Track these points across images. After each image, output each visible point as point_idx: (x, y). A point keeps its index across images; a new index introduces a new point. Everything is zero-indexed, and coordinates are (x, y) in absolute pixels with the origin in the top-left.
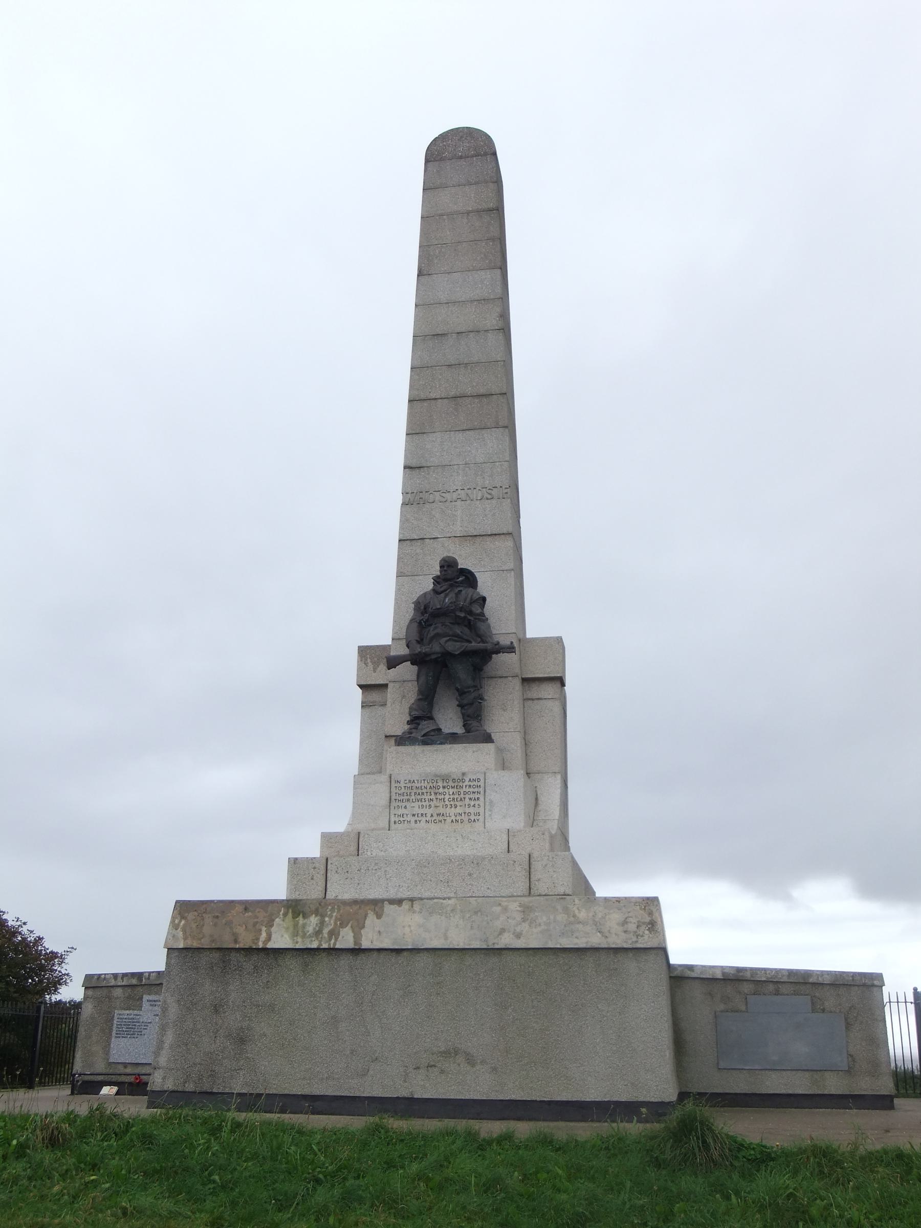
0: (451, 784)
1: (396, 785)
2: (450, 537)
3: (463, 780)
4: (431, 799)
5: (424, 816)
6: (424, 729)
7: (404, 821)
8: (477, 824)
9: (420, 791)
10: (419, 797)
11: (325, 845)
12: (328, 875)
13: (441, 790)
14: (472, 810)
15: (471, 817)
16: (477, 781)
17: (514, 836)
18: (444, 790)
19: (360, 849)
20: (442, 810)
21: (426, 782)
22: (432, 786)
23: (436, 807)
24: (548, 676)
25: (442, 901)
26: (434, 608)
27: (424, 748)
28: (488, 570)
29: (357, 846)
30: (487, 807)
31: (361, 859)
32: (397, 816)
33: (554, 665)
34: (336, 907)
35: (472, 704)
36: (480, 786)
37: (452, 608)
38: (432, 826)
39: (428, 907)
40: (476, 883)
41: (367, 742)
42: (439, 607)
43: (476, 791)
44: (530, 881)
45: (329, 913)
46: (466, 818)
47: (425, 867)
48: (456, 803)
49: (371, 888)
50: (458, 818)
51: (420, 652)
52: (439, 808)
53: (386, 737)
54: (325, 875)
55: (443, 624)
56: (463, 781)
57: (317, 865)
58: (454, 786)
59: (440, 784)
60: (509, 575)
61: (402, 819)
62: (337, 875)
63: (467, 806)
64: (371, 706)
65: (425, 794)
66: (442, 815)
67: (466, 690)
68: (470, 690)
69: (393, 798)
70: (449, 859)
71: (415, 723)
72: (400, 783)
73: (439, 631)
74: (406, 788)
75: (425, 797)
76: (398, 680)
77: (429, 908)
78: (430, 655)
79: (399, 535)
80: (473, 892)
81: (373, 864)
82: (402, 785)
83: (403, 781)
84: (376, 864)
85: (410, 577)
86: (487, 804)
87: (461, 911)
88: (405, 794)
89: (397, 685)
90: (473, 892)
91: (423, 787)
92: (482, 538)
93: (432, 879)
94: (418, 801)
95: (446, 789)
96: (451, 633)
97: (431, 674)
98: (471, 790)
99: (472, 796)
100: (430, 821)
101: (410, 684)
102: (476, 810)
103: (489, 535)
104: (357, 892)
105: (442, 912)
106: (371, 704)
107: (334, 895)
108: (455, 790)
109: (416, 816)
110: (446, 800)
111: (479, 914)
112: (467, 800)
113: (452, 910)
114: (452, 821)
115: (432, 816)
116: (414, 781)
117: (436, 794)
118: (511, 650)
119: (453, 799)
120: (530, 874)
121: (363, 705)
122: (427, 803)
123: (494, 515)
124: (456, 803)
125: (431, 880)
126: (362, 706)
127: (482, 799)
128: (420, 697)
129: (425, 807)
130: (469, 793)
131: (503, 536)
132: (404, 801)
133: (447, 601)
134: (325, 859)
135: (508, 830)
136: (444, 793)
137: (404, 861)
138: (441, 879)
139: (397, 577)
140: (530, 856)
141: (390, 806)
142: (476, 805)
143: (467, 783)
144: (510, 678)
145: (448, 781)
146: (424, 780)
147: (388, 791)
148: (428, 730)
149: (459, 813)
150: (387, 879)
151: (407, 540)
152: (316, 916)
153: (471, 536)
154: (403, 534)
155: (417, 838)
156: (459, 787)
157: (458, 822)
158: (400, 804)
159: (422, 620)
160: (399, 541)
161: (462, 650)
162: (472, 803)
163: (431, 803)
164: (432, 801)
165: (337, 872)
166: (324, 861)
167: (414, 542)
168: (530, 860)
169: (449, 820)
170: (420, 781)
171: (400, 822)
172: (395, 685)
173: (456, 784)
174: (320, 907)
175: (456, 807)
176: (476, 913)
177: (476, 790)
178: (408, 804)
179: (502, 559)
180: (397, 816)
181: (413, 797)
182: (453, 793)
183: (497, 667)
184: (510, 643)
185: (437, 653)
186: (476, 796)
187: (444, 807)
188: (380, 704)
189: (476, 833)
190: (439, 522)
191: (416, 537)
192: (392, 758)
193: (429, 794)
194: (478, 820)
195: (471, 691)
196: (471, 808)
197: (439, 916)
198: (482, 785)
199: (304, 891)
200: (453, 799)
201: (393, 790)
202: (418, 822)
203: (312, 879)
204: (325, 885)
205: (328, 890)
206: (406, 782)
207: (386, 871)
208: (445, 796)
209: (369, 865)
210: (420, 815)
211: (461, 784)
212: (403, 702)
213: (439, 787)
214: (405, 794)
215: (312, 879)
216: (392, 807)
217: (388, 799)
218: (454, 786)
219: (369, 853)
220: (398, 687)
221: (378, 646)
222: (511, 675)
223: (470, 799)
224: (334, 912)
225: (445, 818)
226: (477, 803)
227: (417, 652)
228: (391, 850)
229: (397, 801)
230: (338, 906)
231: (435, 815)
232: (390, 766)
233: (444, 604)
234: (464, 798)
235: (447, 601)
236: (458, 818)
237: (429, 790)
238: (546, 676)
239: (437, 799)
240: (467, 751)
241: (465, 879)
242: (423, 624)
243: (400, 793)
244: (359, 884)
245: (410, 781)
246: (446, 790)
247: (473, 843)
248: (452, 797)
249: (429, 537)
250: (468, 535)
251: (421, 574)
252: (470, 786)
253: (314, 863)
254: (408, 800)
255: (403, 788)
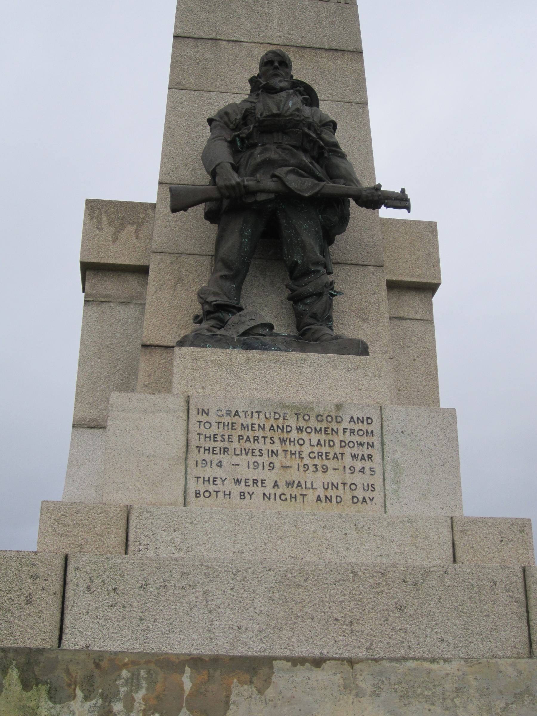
0: (313, 423)
1: (200, 418)
2: (261, 43)
3: (339, 419)
4: (272, 451)
5: (259, 484)
6: (244, 322)
7: (217, 492)
8: (368, 507)
9: (250, 433)
10: (248, 445)
11: (50, 530)
12: (67, 595)
13: (294, 435)
14: (358, 479)
15: (356, 493)
16: (365, 422)
17: (464, 531)
18: (301, 436)
19: (131, 542)
20: (295, 475)
21: (262, 416)
22: (275, 426)
23: (285, 467)
24: (418, 280)
25: (427, 665)
26: (266, 113)
27: (251, 356)
28: (327, 98)
29: (124, 535)
30: (389, 475)
31: (148, 562)
32: (201, 480)
33: (427, 264)
34: (142, 672)
35: (320, 295)
36: (372, 432)
37: (298, 118)
38: (278, 505)
39: (393, 679)
40: (413, 628)
41: (93, 363)
42: (275, 111)
43: (366, 441)
44: (529, 625)
45: (123, 690)
46: (347, 496)
47: (298, 586)
48: (326, 462)
49: (171, 631)
50: (331, 493)
51: (238, 184)
52: (288, 471)
53: (144, 346)
54: (59, 595)
55: (279, 145)
56: (338, 420)
57: (41, 570)
58: (321, 429)
59: (292, 422)
60: (360, 111)
61: (212, 488)
62: (89, 597)
63: (348, 471)
64: (102, 302)
65: (261, 440)
66: (298, 486)
67: (313, 268)
68: (319, 268)
69: (194, 443)
70: (352, 572)
71: (214, 318)
72: (207, 415)
73: (273, 154)
74: (221, 425)
75: (257, 446)
76: (168, 250)
77: (399, 683)
78: (254, 193)
79: (175, 30)
80: (410, 647)
81: (177, 575)
82: (213, 418)
83: (215, 411)
84: (184, 575)
85: (193, 92)
86: (388, 468)
87: (482, 695)
88: (219, 438)
89: (168, 259)
90: (410, 647)
91: (256, 427)
92: (314, 51)
93: (314, 615)
94: (247, 454)
95: (304, 433)
96: (293, 161)
97: (248, 233)
98: (356, 438)
99: (356, 450)
100: (272, 496)
101: (191, 260)
102: (367, 479)
103: (326, 49)
104: (137, 639)
105: (433, 694)
106: (103, 300)
107: (81, 643)
108: (323, 437)
109: (243, 483)
110: (305, 455)
111: (527, 700)
112: (348, 461)
113: (458, 691)
114: (319, 499)
115: (276, 485)
116: (237, 413)
117: (283, 441)
118: (403, 204)
119: (320, 455)
120: (528, 612)
121: (86, 300)
122: (265, 459)
123: (332, 23)
124: (326, 462)
125: (312, 619)
126: (85, 301)
127: (377, 457)
128: (224, 272)
129: (261, 467)
130: (351, 444)
131: (348, 53)
132: (218, 451)
133: (290, 105)
134: (62, 557)
135: (452, 518)
136: (301, 442)
137: (250, 571)
138: (336, 616)
139: (169, 88)
140: (524, 570)
141: (186, 459)
142: (367, 470)
143: (345, 424)
144: (371, 268)
145: (306, 418)
146: (258, 412)
147: (184, 427)
148: (253, 324)
149: (333, 484)
150: (210, 612)
151: (188, 38)
152: (87, 698)
153: (296, 46)
154: (182, 28)
155: (258, 526)
156: (329, 431)
157: (331, 501)
158: (208, 457)
159: (238, 136)
160: (176, 37)
161: (314, 191)
162: (359, 465)
163: (274, 459)
164: (277, 455)
165: (89, 588)
166: (60, 562)
167: (199, 42)
168: (525, 580)
169: (311, 496)
170: (250, 413)
171: (207, 494)
172: (164, 258)
173: (324, 425)
174: (97, 672)
175: (325, 470)
176: (519, 697)
177: (365, 439)
178: (225, 459)
179: (348, 86)
180: (201, 480)
181: (236, 445)
182: (319, 443)
183: (348, 246)
184: (399, 192)
185: (269, 192)
186: (366, 451)
187: (302, 469)
188: (120, 300)
189: (385, 522)
190: (244, 20)
191: (203, 36)
192: (185, 368)
193: (268, 440)
194: (371, 500)
195: (319, 271)
196: (357, 474)
197: (427, 706)
198: (377, 431)
199: (7, 629)
200: (320, 455)
201: (194, 427)
202: (247, 496)
203: (28, 602)
204: (58, 619)
205: (67, 630)
206: (220, 413)
207: (207, 592)
208: (303, 448)
209: (166, 576)
210: (250, 483)
211: (334, 425)
212: (179, 290)
213: (289, 429)
214: (219, 438)
215: (28, 602)
216: (191, 463)
217: (183, 444)
218: (321, 429)
219: (151, 554)
220: (169, 262)
221: (121, 203)
222: (372, 264)
223: (354, 457)
224: (138, 687)
225: (304, 493)
226: (368, 465)
227: (233, 182)
228: (202, 549)
229: (202, 450)
230: (149, 672)
231: (282, 484)
232: (180, 383)
233: (285, 108)
234: (342, 454)
235: (290, 105)
236: (331, 493)
237: (269, 434)
238: (414, 280)
239: (285, 451)
240: (336, 368)
241: (390, 619)
242: (239, 144)
243: (208, 435)
244: (141, 619)
245: (228, 413)
246: (304, 435)
247: (379, 542)
248: (316, 449)
249: (227, 38)
250: (292, 44)
251: (210, 89)
252: (352, 431)
253: (33, 565)
254: (226, 450)
255: (214, 426)
